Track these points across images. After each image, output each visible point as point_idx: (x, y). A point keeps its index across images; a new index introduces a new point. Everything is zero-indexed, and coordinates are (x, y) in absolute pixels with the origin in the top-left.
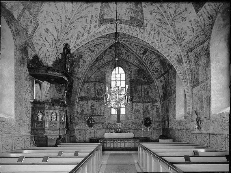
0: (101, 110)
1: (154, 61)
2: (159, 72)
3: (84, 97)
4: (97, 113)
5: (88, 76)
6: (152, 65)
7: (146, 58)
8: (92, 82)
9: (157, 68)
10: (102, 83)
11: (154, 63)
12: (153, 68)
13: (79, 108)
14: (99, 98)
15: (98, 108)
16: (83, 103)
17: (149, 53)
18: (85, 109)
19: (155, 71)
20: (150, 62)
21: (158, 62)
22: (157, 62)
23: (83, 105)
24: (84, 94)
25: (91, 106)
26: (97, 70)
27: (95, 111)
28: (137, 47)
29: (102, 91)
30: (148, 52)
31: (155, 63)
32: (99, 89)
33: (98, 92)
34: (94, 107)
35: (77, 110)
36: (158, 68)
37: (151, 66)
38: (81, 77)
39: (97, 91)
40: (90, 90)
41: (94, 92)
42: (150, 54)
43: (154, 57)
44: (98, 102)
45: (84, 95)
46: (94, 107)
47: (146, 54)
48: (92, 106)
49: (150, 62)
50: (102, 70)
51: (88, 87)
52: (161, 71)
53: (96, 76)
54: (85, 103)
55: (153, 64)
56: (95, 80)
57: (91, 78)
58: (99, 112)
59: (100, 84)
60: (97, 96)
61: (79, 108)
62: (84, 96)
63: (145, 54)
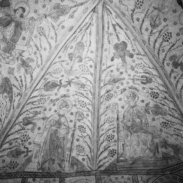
1: (40, 123)
2: (22, 159)
6: (23, 129)
7: (35, 99)
9: (27, 146)
11: (32, 130)
12: (18, 136)
17: (54, 97)
19: (15, 148)
20: (31, 115)
21: (45, 134)
22: (41, 131)
28: (67, 58)
30: (55, 90)
31: (36, 130)
36: (30, 147)
37: (17, 127)
42: (51, 101)
43: (48, 114)
47: (46, 93)
49: (30, 118)
52: (29, 161)
55: (30, 126)
63: (47, 91)
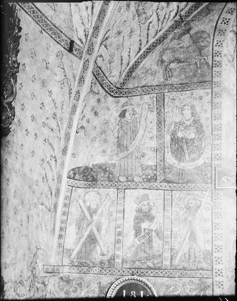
0: (193, 237)
3: (104, 168)
4: (167, 255)
5: (125, 55)
8: (147, 89)
10: (200, 92)
13: (72, 230)
14: (181, 173)
15: (175, 229)
16: (91, 197)
18: (103, 232)
23: (92, 212)
24: (104, 151)
25: (134, 214)
26: (172, 28)
27: (157, 243)
29: (200, 130)
32: (181, 123)
33: (175, 140)
34: (151, 218)
35: (60, 236)
38: (81, 34)
39: (174, 134)
40: (135, 132)
41: (154, 144)
44: (176, 194)
45: (100, 160)
46: (151, 218)
48: (144, 215)
50: (202, 28)
51: (123, 115)
53: (165, 58)
54: (107, 203)
56: (159, 78)
57: (138, 71)
58: (185, 248)
59: (185, 97)
60: (170, 159)
61: (72, 230)
62: (100, 167)
